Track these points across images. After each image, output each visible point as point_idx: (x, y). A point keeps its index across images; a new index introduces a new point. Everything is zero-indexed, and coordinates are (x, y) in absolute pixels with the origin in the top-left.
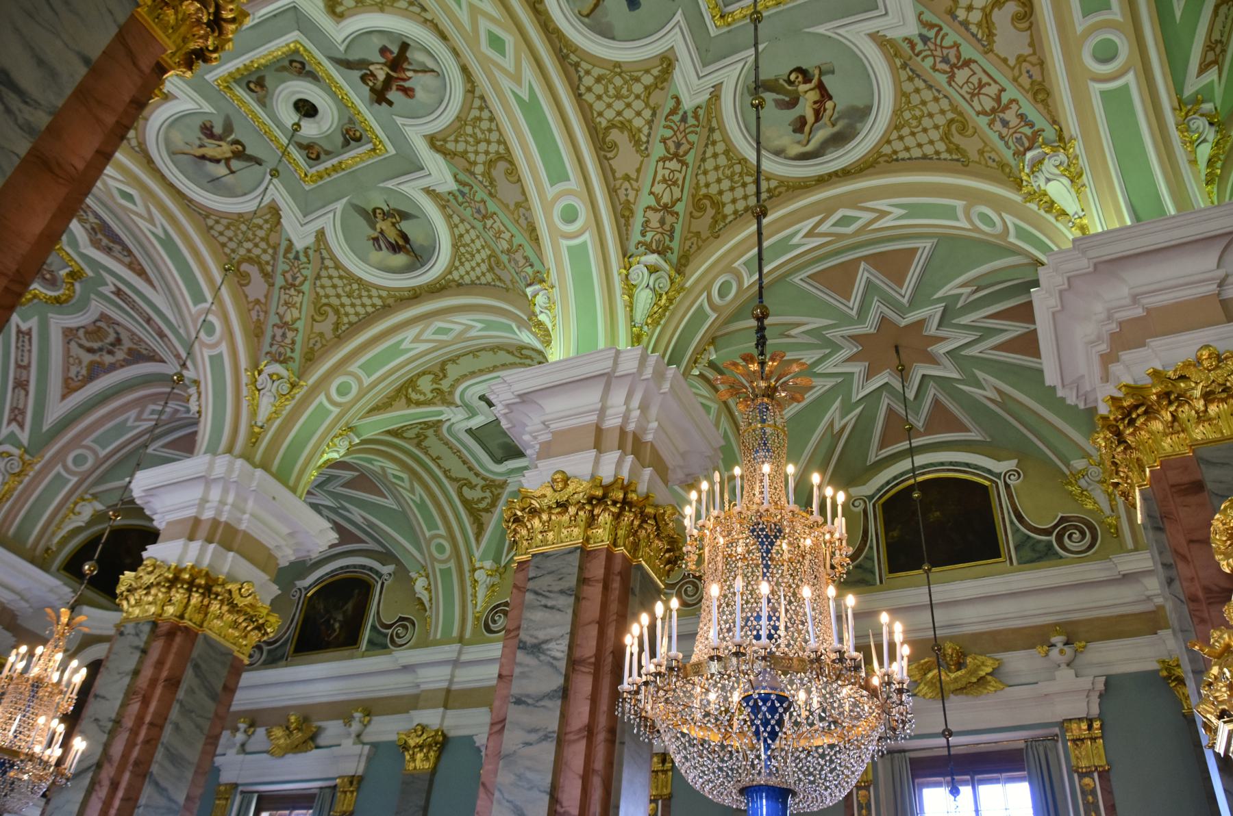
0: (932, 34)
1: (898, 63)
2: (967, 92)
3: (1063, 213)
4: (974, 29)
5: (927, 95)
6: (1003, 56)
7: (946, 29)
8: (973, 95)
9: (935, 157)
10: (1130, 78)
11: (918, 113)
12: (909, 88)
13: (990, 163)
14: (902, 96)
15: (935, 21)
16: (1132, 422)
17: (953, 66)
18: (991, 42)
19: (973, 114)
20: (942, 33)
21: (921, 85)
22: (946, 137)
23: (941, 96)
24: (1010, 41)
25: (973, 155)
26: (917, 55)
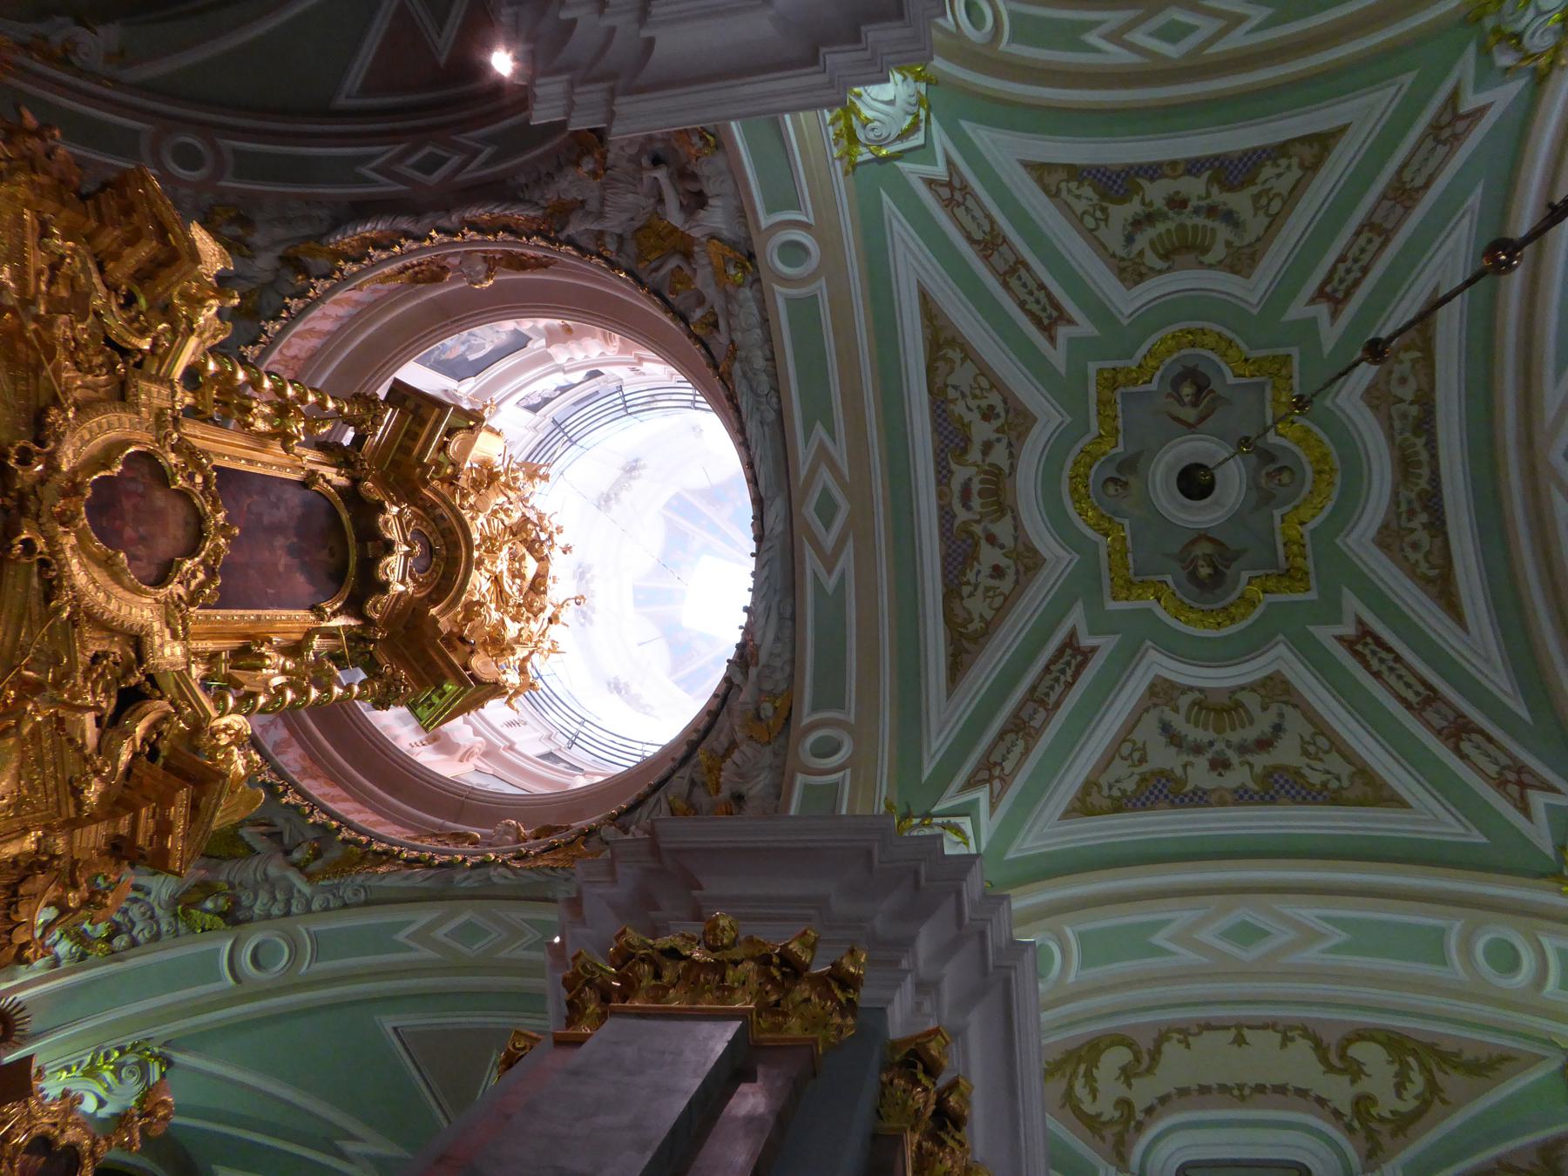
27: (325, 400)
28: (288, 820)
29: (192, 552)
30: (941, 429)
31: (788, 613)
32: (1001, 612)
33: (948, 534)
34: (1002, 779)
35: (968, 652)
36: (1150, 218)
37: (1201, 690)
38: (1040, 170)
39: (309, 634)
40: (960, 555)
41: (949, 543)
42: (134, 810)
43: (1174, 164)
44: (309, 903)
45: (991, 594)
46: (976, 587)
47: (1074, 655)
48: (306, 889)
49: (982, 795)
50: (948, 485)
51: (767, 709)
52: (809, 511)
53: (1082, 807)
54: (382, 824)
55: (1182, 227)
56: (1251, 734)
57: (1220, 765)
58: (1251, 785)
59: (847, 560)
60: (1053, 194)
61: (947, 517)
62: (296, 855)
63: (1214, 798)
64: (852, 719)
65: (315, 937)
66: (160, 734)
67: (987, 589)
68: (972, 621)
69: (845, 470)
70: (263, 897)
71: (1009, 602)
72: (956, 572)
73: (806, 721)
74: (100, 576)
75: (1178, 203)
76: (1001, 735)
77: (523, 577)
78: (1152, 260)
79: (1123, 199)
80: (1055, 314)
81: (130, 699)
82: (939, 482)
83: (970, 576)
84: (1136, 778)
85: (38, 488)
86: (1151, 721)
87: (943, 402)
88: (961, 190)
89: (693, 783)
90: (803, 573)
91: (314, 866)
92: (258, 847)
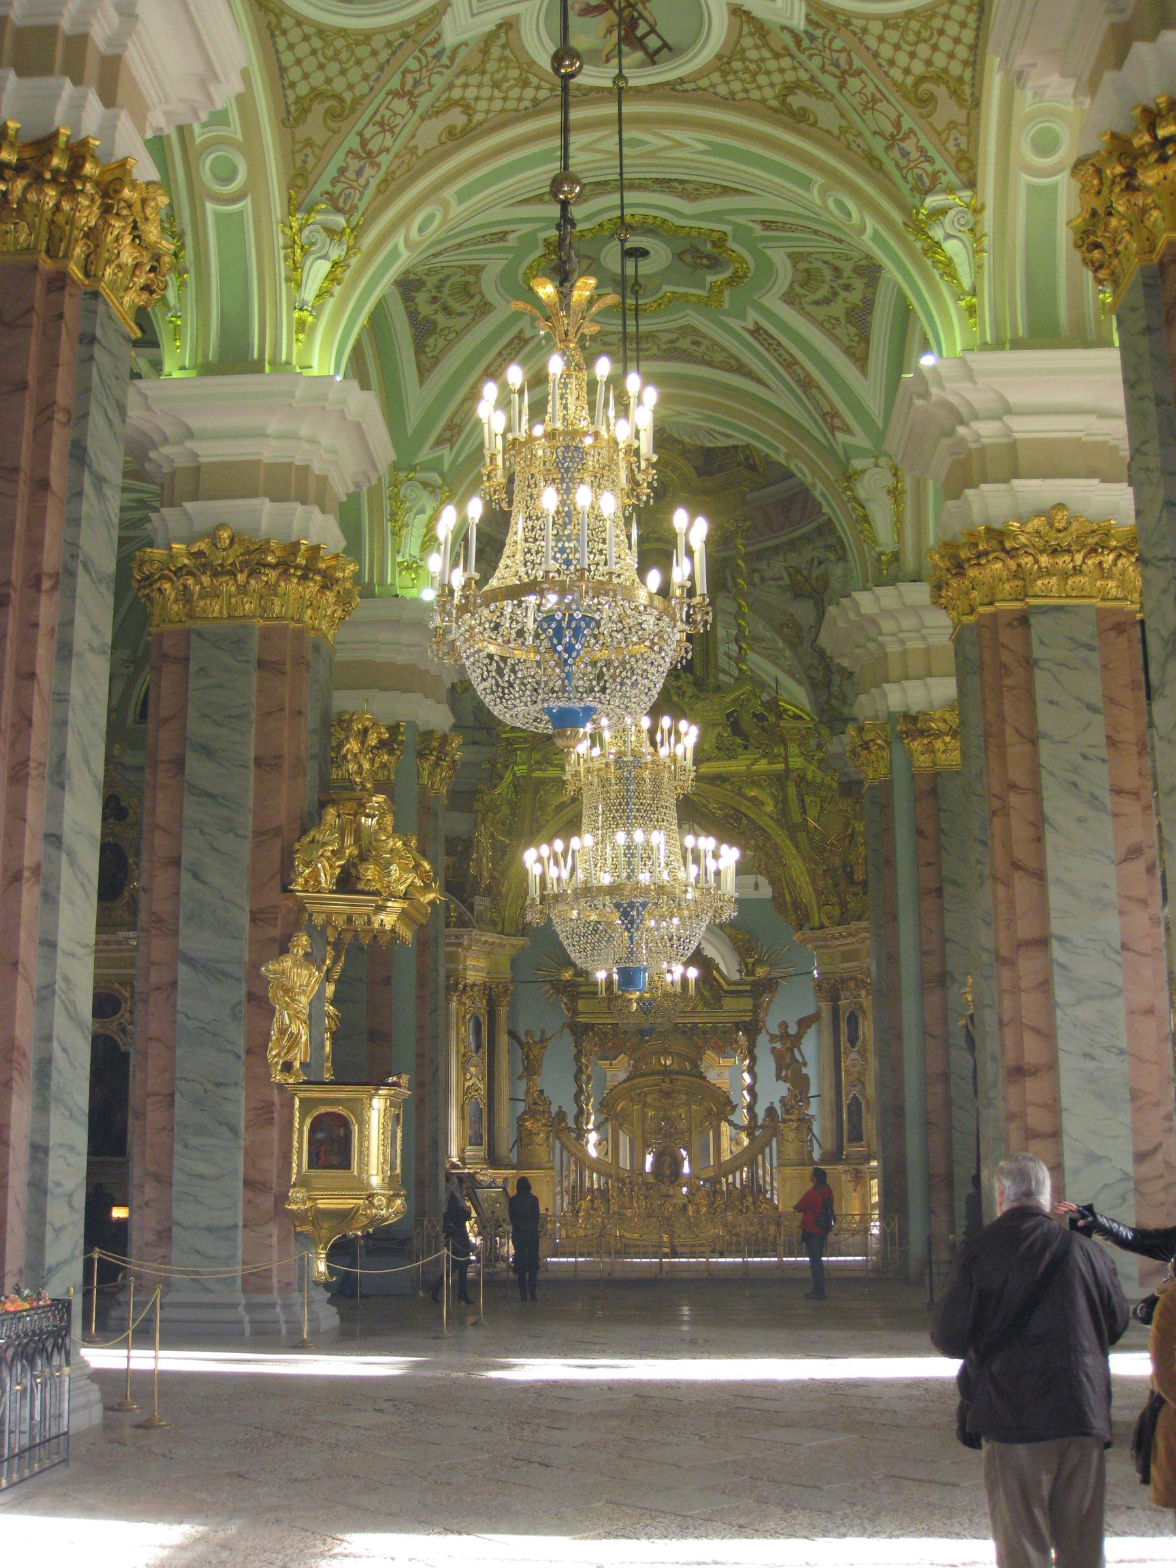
0: (445, 60)
1: (410, 29)
2: (383, 116)
3: (299, 286)
4: (444, 97)
5: (370, 66)
6: (418, 133)
7: (447, 72)
8: (381, 124)
9: (286, 83)
10: (405, 254)
11: (344, 56)
12: (378, 42)
13: (299, 157)
14: (367, 36)
15: (458, 60)
16: (304, 578)
17: (410, 93)
18: (430, 117)
19: (359, 127)
20: (444, 70)
21: (384, 55)
22: (317, 95)
23: (372, 83)
24: (430, 134)
25: (303, 132)
26: (421, 51)
32: (723, 349)
34: (833, 418)
36: (447, 311)
37: (793, 282)
38: (423, 372)
43: (406, 307)
47: (757, 331)
53: (861, 361)
55: (451, 295)
56: (828, 273)
57: (847, 288)
58: (866, 280)
60: (437, 360)
63: (869, 296)
64: (786, 451)
71: (715, 343)
75: (434, 300)
78: (476, 301)
79: (435, 323)
80: (516, 341)
84: (848, 326)
86: (811, 309)
88: (452, 430)
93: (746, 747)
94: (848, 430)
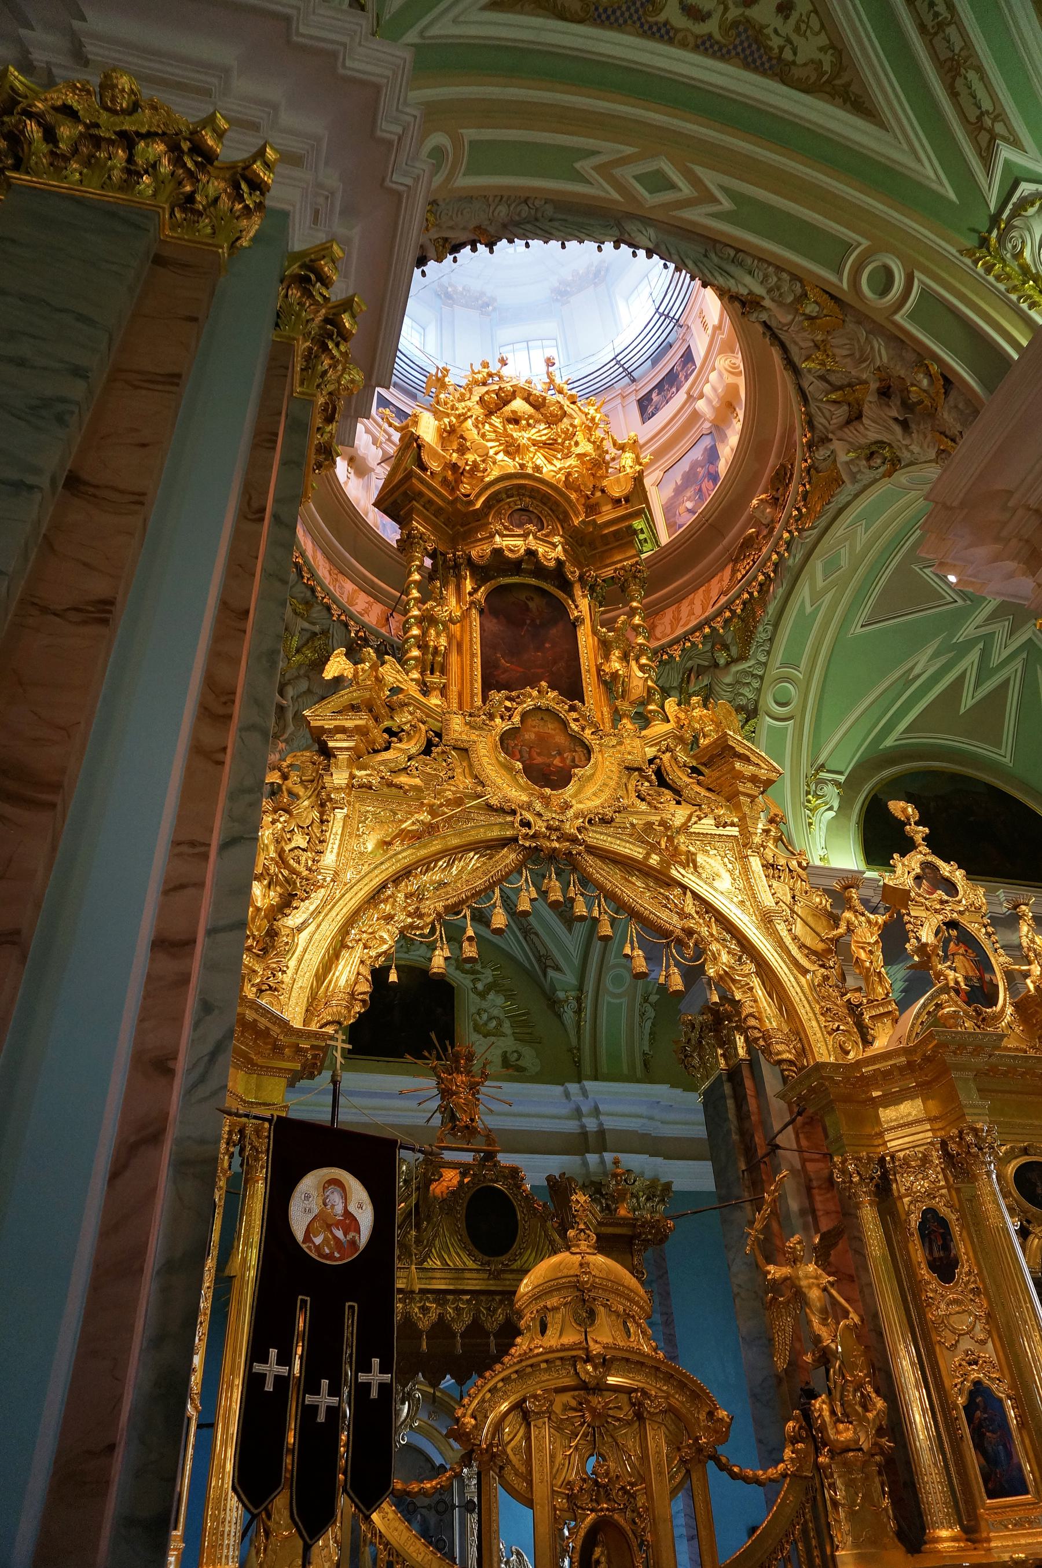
27: (415, 582)
28: (690, 659)
29: (565, 724)
30: (621, 21)
31: (732, 253)
33: (724, 50)
34: (994, 120)
35: (848, 85)
39: (595, 632)
40: (750, 46)
41: (733, 53)
42: (738, 793)
44: (760, 663)
45: (803, 27)
46: (789, 41)
48: (752, 662)
49: (1006, 153)
50: (677, 31)
51: (811, 309)
52: (650, 199)
54: (708, 591)
59: (709, 178)
61: (708, 44)
62: (722, 662)
64: (865, 243)
65: (784, 665)
66: (685, 766)
67: (797, 29)
68: (820, 61)
69: (629, 150)
70: (745, 691)
72: (765, 58)
73: (845, 286)
74: (590, 790)
76: (954, 94)
77: (531, 417)
81: (662, 780)
82: (671, 41)
83: (775, 42)
85: (545, 818)
87: (597, 9)
89: (822, 378)
90: (705, 227)
91: (734, 651)
92: (706, 682)
93: (678, 803)
94: (1016, 143)
